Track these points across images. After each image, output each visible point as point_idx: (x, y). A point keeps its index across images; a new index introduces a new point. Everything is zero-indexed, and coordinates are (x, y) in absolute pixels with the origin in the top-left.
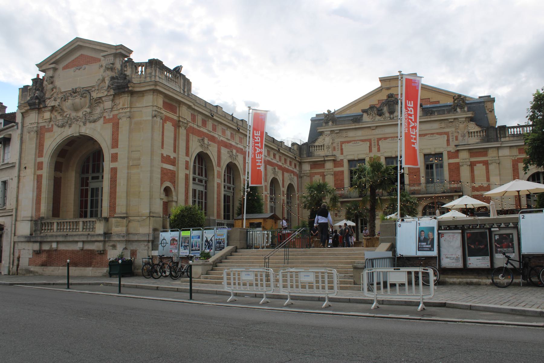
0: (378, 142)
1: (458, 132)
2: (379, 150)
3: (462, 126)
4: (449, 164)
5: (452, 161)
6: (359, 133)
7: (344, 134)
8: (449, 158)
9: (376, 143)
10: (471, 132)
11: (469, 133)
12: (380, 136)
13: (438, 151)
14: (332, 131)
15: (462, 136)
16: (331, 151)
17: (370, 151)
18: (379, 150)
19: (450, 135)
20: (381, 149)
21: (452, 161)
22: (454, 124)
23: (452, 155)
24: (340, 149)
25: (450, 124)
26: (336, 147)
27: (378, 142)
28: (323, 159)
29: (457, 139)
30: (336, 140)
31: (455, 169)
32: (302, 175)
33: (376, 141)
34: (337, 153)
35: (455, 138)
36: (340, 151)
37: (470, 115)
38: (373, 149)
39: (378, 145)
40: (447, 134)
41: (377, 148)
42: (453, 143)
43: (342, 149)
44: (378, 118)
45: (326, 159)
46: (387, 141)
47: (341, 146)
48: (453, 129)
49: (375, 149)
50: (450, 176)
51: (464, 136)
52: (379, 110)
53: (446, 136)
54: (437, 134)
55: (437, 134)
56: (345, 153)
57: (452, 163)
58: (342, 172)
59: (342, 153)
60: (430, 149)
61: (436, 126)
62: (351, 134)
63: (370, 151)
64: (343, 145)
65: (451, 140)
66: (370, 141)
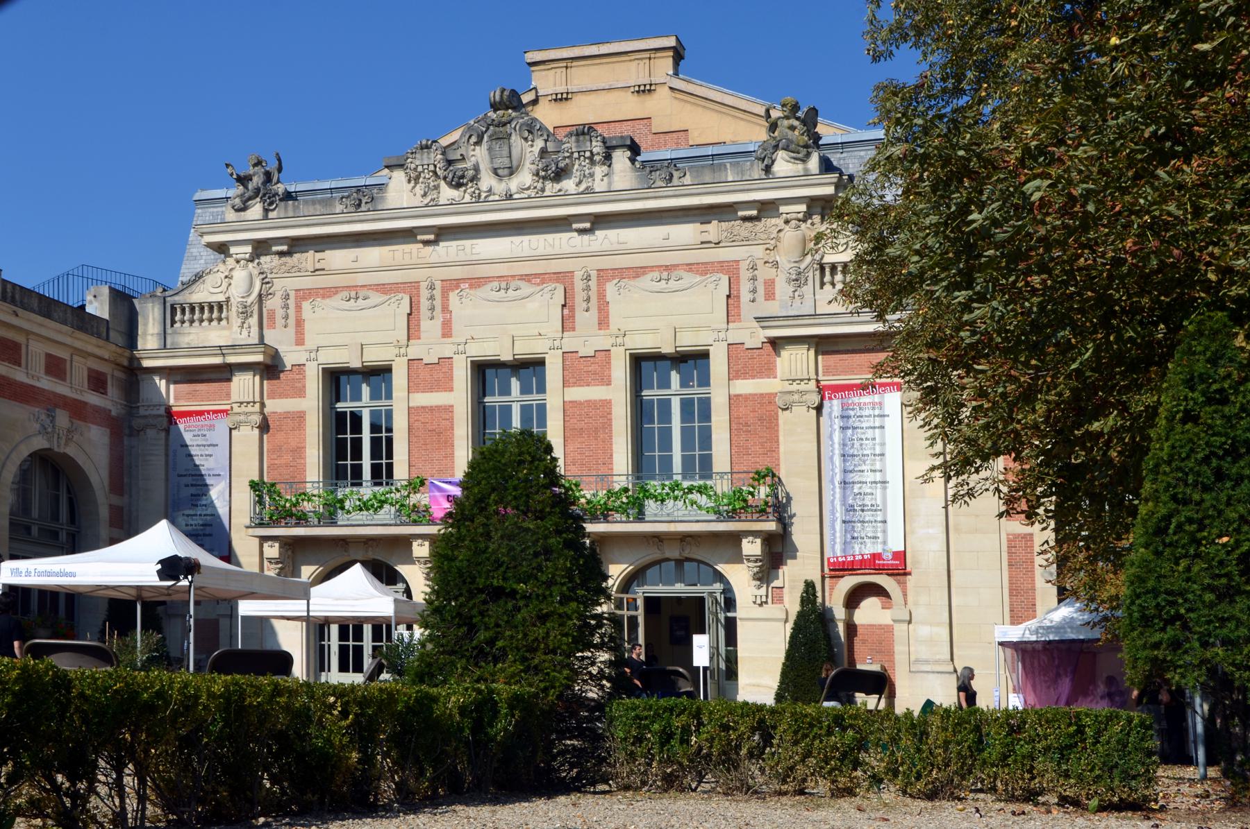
0: (445, 297)
1: (776, 265)
2: (447, 331)
3: (790, 236)
4: (733, 400)
5: (745, 386)
6: (372, 255)
7: (308, 259)
8: (734, 374)
9: (438, 303)
10: (833, 267)
11: (822, 269)
12: (457, 273)
13: (688, 341)
14: (261, 248)
15: (789, 281)
16: (255, 330)
17: (412, 331)
18: (447, 331)
19: (745, 275)
20: (456, 327)
21: (745, 386)
22: (760, 225)
23: (745, 362)
24: (292, 321)
25: (744, 229)
26: (280, 313)
27: (445, 297)
28: (218, 360)
29: (770, 295)
30: (279, 285)
31: (758, 420)
32: (137, 423)
33: (437, 293)
34: (279, 338)
35: (761, 290)
36: (292, 329)
37: (830, 190)
38: (425, 324)
39: (445, 309)
40: (730, 269)
41: (438, 322)
42: (748, 310)
43: (300, 323)
44: (447, 193)
45: (232, 359)
46: (486, 291)
47: (299, 308)
48: (759, 252)
49: (430, 327)
50: (737, 451)
51: (798, 280)
52: (450, 163)
53: (725, 279)
54: (690, 267)
55: (690, 267)
56: (311, 341)
57: (746, 398)
58: (300, 417)
59: (300, 341)
60: (655, 330)
61: (686, 232)
62: (337, 258)
63: (412, 331)
64: (306, 305)
65: (745, 296)
66: (412, 289)
